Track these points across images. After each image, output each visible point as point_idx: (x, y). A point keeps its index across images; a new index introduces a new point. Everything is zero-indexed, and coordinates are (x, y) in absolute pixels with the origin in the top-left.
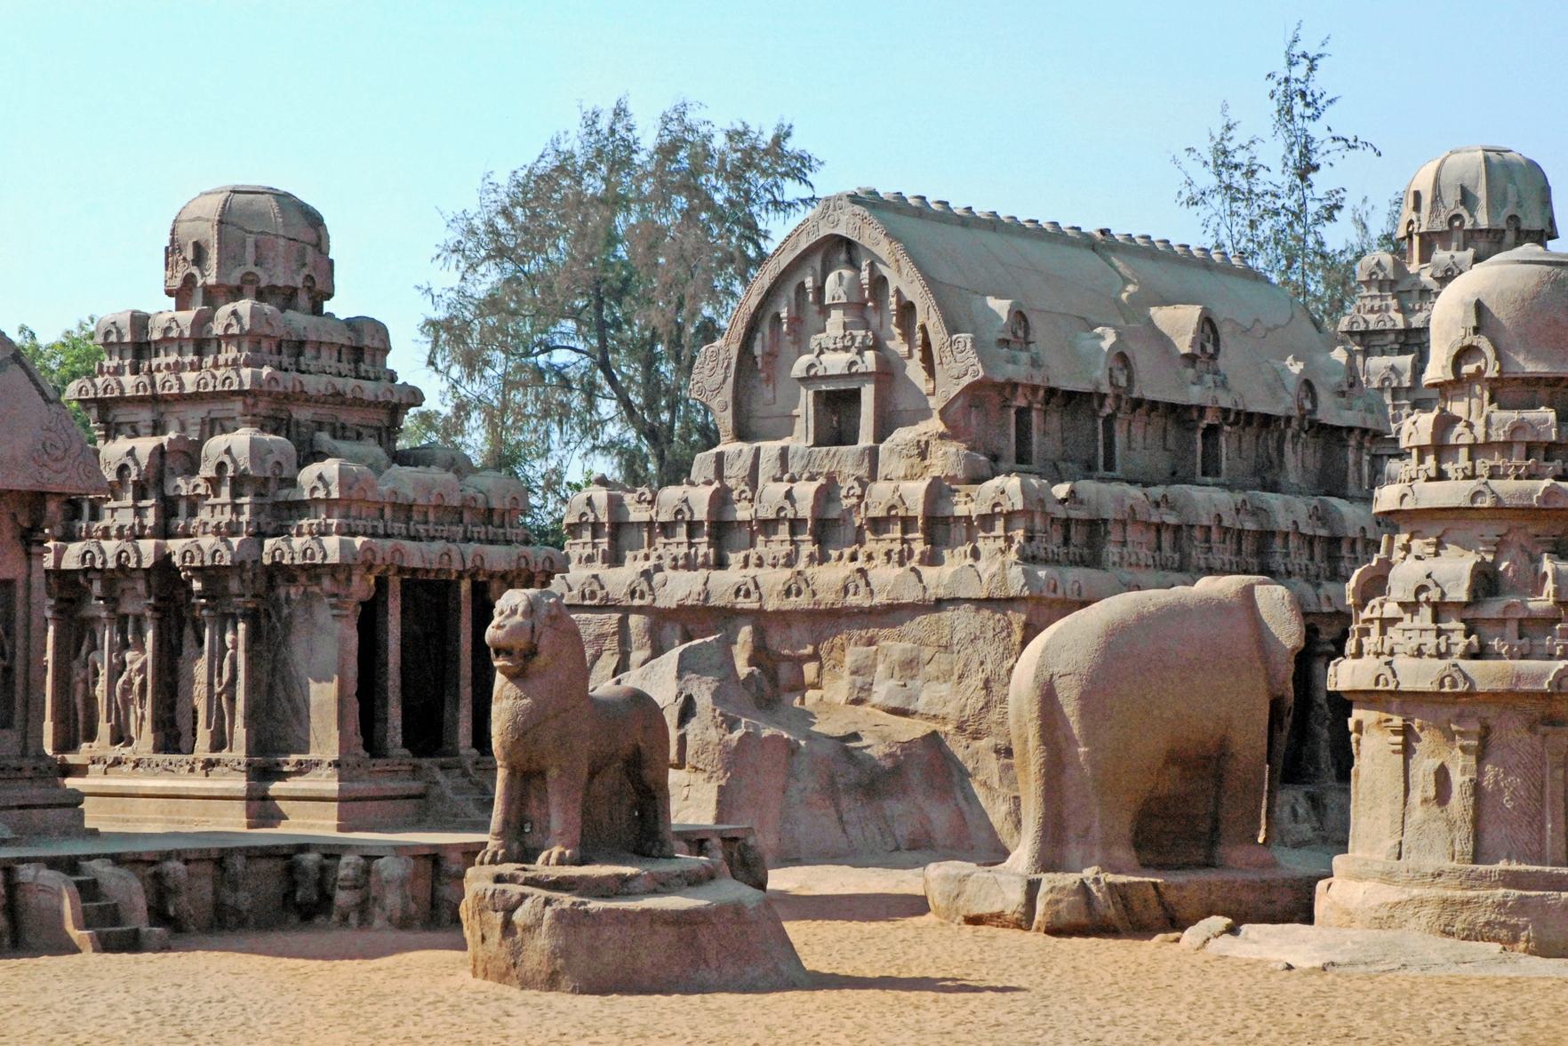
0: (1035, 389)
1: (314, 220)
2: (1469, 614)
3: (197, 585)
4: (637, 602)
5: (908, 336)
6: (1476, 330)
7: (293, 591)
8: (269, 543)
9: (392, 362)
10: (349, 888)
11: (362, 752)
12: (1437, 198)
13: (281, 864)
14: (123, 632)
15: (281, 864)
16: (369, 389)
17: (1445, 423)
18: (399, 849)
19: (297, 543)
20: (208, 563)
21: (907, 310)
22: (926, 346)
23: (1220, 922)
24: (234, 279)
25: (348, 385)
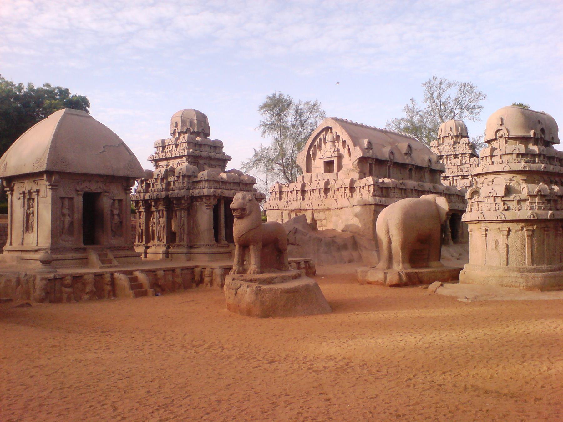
0: (373, 159)
1: (205, 117)
2: (504, 199)
3: (175, 202)
4: (285, 208)
5: (344, 148)
6: (501, 125)
8: (191, 191)
9: (224, 150)
11: (215, 242)
12: (445, 130)
13: (190, 271)
14: (159, 213)
15: (190, 271)
16: (218, 156)
17: (493, 149)
18: (220, 267)
19: (197, 191)
21: (344, 142)
22: (349, 150)
23: (437, 283)
25: (212, 155)
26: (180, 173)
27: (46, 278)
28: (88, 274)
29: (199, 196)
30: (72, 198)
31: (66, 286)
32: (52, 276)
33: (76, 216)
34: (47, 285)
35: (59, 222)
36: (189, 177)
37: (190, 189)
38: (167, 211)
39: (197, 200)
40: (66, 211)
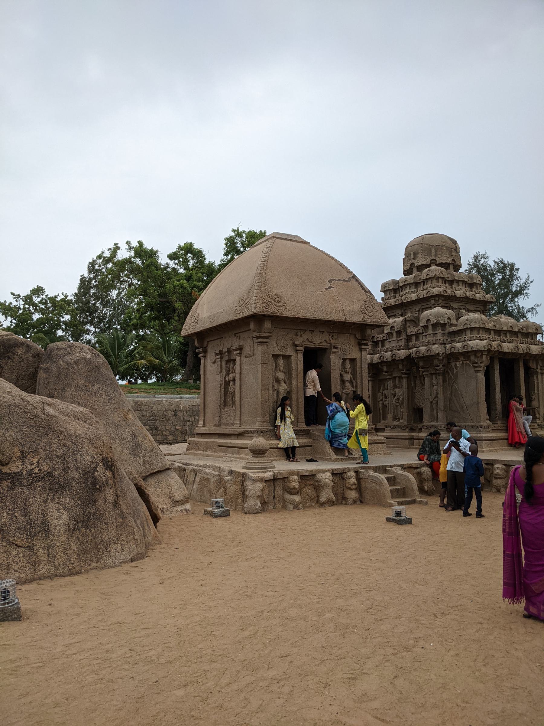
1: (455, 242)
3: (421, 364)
7: (457, 363)
10: (500, 478)
11: (489, 422)
14: (394, 382)
19: (459, 345)
20: (426, 354)
24: (428, 261)
26: (428, 320)
27: (262, 479)
28: (323, 471)
29: (461, 354)
30: (289, 357)
31: (292, 491)
32: (268, 475)
33: (294, 382)
34: (263, 490)
35: (271, 392)
36: (443, 326)
37: (445, 344)
38: (408, 378)
39: (457, 359)
40: (281, 376)
